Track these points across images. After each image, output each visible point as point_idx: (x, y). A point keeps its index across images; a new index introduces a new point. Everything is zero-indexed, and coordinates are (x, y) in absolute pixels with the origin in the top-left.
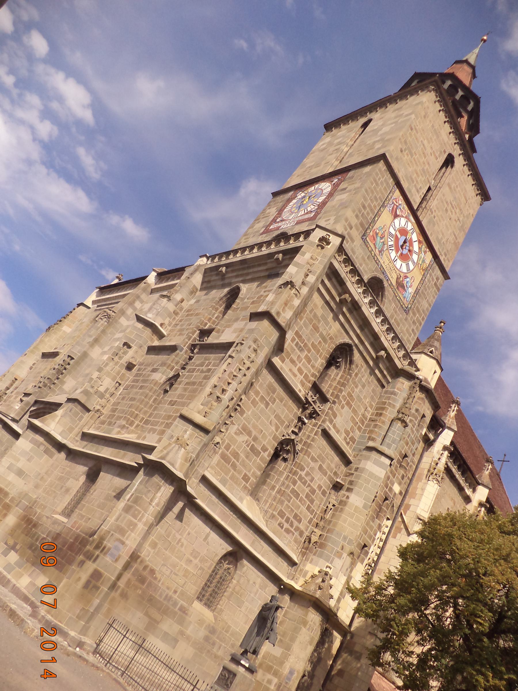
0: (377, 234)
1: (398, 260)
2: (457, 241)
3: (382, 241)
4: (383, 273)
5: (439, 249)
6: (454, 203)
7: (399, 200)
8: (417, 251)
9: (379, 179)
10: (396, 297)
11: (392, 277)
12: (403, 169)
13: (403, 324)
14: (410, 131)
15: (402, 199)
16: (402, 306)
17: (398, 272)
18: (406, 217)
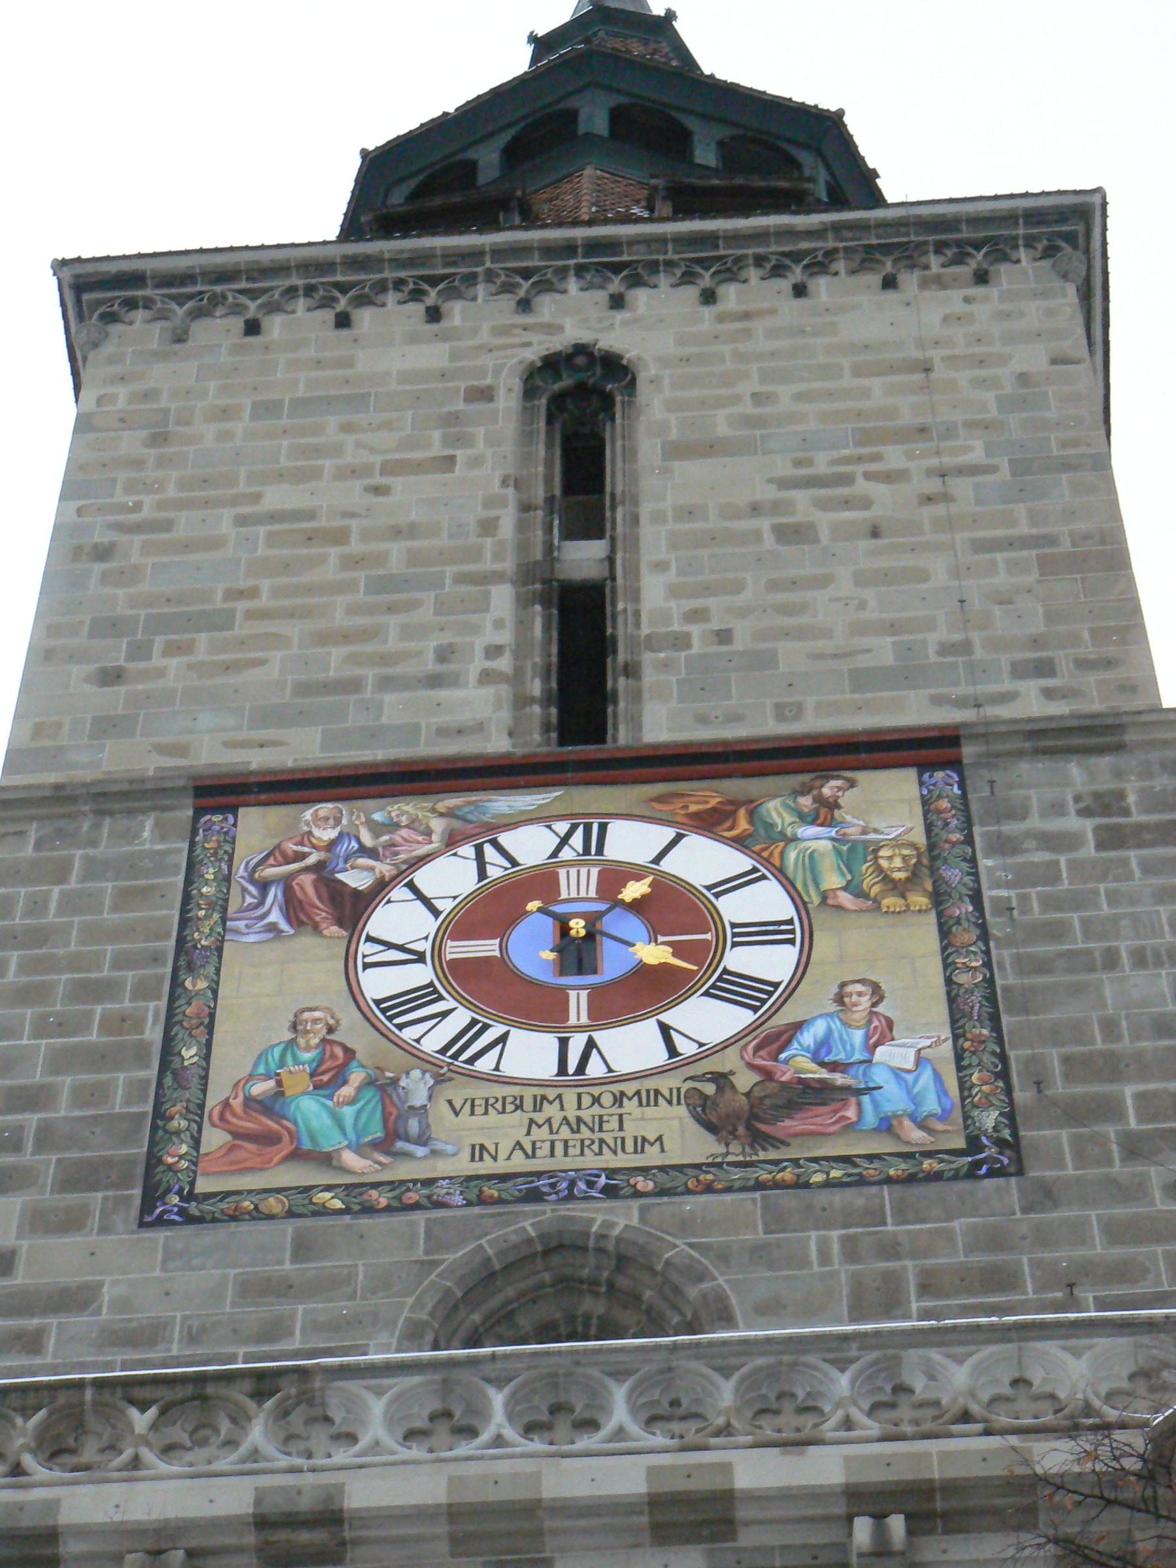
0: (271, 1106)
1: (599, 1037)
2: (1066, 546)
3: (347, 1091)
4: (534, 1196)
5: (937, 701)
6: (822, 465)
8: (741, 862)
9: (37, 906)
10: (802, 1184)
11: (641, 1144)
12: (206, 719)
13: (1044, 1237)
14: (98, 567)
15: (325, 808)
16: (911, 1179)
17: (665, 1084)
18: (452, 842)
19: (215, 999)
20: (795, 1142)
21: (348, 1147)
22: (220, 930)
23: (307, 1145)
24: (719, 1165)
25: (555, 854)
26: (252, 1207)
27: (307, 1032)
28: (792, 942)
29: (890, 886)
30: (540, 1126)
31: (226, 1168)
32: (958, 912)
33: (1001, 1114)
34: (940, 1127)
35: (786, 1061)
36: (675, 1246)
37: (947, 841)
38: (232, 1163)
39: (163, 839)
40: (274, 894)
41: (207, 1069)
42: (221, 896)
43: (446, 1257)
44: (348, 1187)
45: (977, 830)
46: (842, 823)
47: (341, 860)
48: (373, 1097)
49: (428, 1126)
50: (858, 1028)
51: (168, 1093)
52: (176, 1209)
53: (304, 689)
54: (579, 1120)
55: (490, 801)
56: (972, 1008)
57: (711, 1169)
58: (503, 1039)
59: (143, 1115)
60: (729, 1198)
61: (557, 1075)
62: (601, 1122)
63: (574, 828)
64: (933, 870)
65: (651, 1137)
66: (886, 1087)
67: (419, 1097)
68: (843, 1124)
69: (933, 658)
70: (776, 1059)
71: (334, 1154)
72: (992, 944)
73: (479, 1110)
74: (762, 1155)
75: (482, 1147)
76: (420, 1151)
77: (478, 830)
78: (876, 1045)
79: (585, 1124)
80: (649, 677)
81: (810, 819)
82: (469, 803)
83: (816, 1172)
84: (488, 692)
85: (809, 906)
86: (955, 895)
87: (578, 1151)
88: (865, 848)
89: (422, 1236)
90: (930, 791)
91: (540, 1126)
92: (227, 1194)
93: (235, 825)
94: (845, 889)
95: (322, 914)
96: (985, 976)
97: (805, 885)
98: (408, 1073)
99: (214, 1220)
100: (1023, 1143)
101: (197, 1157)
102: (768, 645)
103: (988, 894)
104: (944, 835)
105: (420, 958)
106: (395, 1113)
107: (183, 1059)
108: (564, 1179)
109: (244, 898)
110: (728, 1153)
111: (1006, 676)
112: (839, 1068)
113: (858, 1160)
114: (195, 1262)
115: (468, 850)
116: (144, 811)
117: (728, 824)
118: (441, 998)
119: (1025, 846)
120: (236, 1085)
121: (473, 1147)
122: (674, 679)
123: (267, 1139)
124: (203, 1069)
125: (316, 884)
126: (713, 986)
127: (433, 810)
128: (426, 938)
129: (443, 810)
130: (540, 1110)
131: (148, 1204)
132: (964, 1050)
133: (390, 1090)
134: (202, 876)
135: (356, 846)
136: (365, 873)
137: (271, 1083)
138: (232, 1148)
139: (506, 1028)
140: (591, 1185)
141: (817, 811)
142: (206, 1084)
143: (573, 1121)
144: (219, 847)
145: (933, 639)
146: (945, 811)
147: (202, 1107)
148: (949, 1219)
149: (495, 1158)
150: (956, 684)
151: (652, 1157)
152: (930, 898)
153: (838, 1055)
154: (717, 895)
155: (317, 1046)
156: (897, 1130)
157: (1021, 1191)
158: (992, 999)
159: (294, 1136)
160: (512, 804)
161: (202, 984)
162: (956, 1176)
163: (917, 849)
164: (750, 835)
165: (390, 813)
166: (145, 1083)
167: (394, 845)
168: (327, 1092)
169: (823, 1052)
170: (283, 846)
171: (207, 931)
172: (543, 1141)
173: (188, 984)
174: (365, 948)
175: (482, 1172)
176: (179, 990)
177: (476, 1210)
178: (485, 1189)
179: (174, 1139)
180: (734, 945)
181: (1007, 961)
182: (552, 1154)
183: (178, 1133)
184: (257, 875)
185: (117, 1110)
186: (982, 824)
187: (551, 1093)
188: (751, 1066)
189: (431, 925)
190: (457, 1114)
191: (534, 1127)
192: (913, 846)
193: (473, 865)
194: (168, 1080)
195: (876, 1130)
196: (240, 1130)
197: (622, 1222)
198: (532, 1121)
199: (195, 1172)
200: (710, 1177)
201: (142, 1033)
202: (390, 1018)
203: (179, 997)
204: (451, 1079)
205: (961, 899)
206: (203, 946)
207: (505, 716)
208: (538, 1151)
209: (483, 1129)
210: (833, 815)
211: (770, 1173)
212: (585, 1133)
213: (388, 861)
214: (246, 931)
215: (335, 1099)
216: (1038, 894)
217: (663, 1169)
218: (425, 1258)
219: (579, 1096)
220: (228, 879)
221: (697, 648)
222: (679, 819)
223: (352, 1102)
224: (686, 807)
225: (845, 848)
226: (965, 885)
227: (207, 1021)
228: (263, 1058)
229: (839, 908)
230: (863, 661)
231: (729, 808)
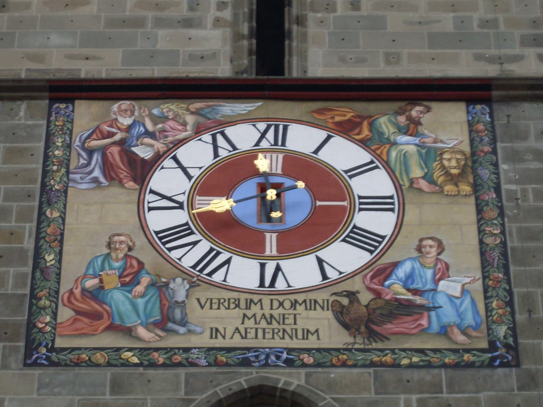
1: (283, 264)
3: (140, 289)
4: (246, 363)
5: (478, 58)
7: (114, 123)
8: (364, 157)
11: (307, 333)
12: (55, 39)
15: (125, 104)
16: (456, 366)
17: (320, 296)
18: (198, 131)
19: (64, 224)
20: (393, 338)
21: (141, 324)
22: (65, 179)
23: (117, 322)
24: (350, 350)
25: (257, 144)
26: (87, 358)
27: (116, 249)
28: (392, 210)
29: (449, 178)
30: (249, 319)
31: (72, 333)
32: (487, 198)
33: (508, 328)
34: (474, 334)
35: (389, 287)
36: (325, 399)
37: (482, 151)
38: (77, 330)
39: (32, 117)
40: (97, 157)
41: (60, 269)
42: (66, 157)
43: (197, 397)
44: (141, 349)
45: (499, 145)
46: (422, 135)
47: (135, 139)
48: (155, 293)
49: (186, 314)
50: (429, 268)
51: (38, 282)
52: (44, 357)
53: (112, 23)
54: (272, 316)
55: (220, 106)
56: (494, 259)
57: (345, 352)
58: (228, 262)
59: (24, 295)
60: (355, 371)
61: (259, 287)
62: (284, 318)
63: (269, 127)
64: (474, 170)
65: (312, 330)
66: (445, 307)
67: (181, 296)
68: (420, 328)
69: (476, 29)
70: (382, 285)
71: (133, 329)
72: (506, 220)
73: (215, 306)
74: (374, 345)
75: (217, 330)
76: (182, 330)
77: (214, 125)
78: (440, 279)
79: (275, 319)
80: (312, 29)
81: (404, 131)
82: (209, 106)
83: (405, 357)
84: (217, 33)
85: (403, 187)
86: (486, 186)
87: (271, 336)
88: (435, 152)
89: (183, 383)
90: (473, 118)
91: (249, 319)
92: (74, 349)
93: (73, 111)
94: (423, 178)
95: (124, 173)
96: (501, 239)
97: (401, 174)
98: (174, 280)
99: (66, 365)
100: (520, 348)
101: (55, 325)
102: (380, 13)
103: (505, 187)
104: (480, 147)
105: (181, 206)
106: (167, 304)
107: (46, 262)
108: (263, 353)
109: (79, 159)
110: (355, 343)
111: (517, 44)
112: (419, 293)
113: (428, 352)
114: (56, 390)
115: (207, 137)
116: (21, 99)
117: (357, 131)
118: (192, 233)
119: (526, 157)
120: (77, 280)
121: (212, 329)
122: (327, 32)
123: (95, 316)
124: (58, 269)
125: (120, 152)
126: (348, 236)
127: (188, 110)
128: (184, 193)
129: (193, 110)
130: (250, 309)
131: (28, 353)
132: (489, 286)
133: (164, 289)
134: (54, 144)
135: (144, 130)
136: (149, 149)
137: (96, 281)
138: (75, 320)
139: (230, 255)
140: (278, 358)
141: (408, 125)
142: (59, 279)
143: (268, 316)
144: (64, 125)
145: (476, 16)
146: (481, 131)
147: (57, 292)
148: (477, 392)
149: (224, 337)
150: (489, 48)
151: (312, 342)
152: (472, 187)
153: (418, 285)
154: (351, 177)
155: (122, 259)
156: (451, 335)
157: (518, 377)
158: (504, 254)
159: (110, 315)
160: (234, 109)
161: (56, 214)
162: (482, 366)
163: (465, 155)
164: (370, 139)
165: (162, 109)
166: (25, 275)
167: (165, 131)
168: (128, 288)
169: (410, 282)
170: (101, 127)
171: (58, 179)
172: (251, 328)
173: (48, 213)
174: (149, 197)
175: (217, 345)
176: (43, 217)
177: (214, 369)
178: (218, 356)
179: (42, 312)
180: (360, 210)
181: (514, 230)
182: (256, 337)
183: (44, 308)
184: (86, 145)
185: (10, 292)
186: (502, 142)
187: (256, 298)
188: (369, 289)
189: (187, 185)
190: (202, 307)
191: (246, 319)
192: (462, 153)
193: (211, 147)
194: (38, 274)
195: (438, 334)
196: (80, 310)
197: (296, 382)
198: (245, 315)
199: (54, 334)
200: (345, 357)
201: (22, 243)
202: (164, 244)
203: (43, 222)
204: (199, 285)
205: (489, 189)
206: (56, 189)
207: (228, 48)
208: (248, 334)
209: (217, 318)
210: (417, 130)
211: (379, 357)
212: (275, 325)
213: (162, 141)
214: (80, 181)
215: (133, 293)
216: (533, 189)
217: (318, 350)
218: (186, 397)
219: (272, 300)
220: (69, 146)
221: (339, 13)
222: (330, 125)
223: (143, 296)
224: (332, 118)
225: (424, 151)
226: (491, 180)
227: (59, 238)
228: (92, 264)
229: (420, 190)
230: (436, 28)
231: (358, 120)
